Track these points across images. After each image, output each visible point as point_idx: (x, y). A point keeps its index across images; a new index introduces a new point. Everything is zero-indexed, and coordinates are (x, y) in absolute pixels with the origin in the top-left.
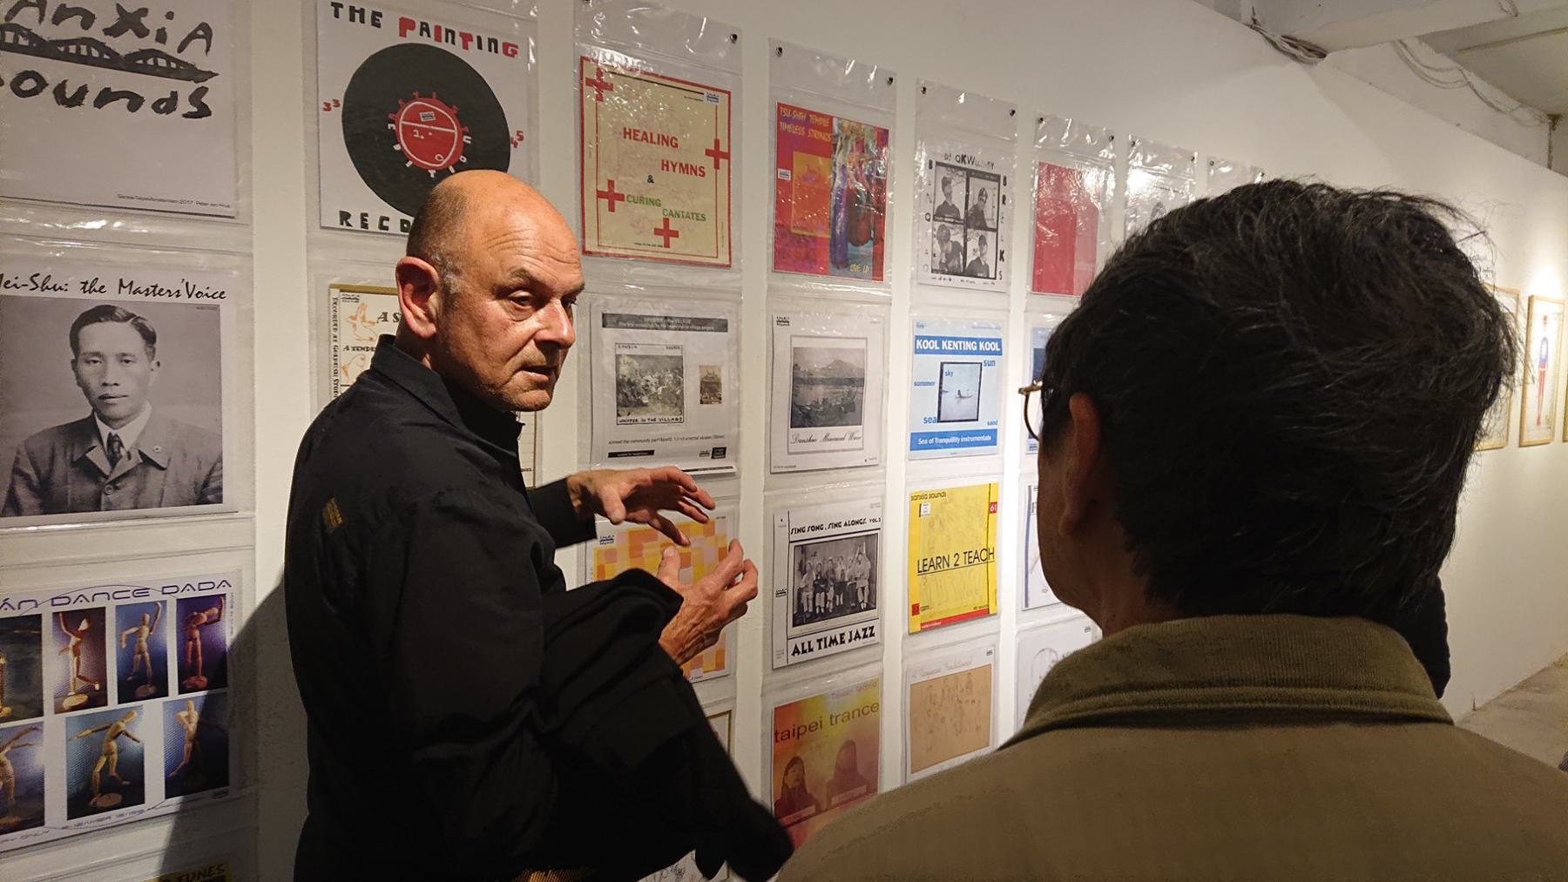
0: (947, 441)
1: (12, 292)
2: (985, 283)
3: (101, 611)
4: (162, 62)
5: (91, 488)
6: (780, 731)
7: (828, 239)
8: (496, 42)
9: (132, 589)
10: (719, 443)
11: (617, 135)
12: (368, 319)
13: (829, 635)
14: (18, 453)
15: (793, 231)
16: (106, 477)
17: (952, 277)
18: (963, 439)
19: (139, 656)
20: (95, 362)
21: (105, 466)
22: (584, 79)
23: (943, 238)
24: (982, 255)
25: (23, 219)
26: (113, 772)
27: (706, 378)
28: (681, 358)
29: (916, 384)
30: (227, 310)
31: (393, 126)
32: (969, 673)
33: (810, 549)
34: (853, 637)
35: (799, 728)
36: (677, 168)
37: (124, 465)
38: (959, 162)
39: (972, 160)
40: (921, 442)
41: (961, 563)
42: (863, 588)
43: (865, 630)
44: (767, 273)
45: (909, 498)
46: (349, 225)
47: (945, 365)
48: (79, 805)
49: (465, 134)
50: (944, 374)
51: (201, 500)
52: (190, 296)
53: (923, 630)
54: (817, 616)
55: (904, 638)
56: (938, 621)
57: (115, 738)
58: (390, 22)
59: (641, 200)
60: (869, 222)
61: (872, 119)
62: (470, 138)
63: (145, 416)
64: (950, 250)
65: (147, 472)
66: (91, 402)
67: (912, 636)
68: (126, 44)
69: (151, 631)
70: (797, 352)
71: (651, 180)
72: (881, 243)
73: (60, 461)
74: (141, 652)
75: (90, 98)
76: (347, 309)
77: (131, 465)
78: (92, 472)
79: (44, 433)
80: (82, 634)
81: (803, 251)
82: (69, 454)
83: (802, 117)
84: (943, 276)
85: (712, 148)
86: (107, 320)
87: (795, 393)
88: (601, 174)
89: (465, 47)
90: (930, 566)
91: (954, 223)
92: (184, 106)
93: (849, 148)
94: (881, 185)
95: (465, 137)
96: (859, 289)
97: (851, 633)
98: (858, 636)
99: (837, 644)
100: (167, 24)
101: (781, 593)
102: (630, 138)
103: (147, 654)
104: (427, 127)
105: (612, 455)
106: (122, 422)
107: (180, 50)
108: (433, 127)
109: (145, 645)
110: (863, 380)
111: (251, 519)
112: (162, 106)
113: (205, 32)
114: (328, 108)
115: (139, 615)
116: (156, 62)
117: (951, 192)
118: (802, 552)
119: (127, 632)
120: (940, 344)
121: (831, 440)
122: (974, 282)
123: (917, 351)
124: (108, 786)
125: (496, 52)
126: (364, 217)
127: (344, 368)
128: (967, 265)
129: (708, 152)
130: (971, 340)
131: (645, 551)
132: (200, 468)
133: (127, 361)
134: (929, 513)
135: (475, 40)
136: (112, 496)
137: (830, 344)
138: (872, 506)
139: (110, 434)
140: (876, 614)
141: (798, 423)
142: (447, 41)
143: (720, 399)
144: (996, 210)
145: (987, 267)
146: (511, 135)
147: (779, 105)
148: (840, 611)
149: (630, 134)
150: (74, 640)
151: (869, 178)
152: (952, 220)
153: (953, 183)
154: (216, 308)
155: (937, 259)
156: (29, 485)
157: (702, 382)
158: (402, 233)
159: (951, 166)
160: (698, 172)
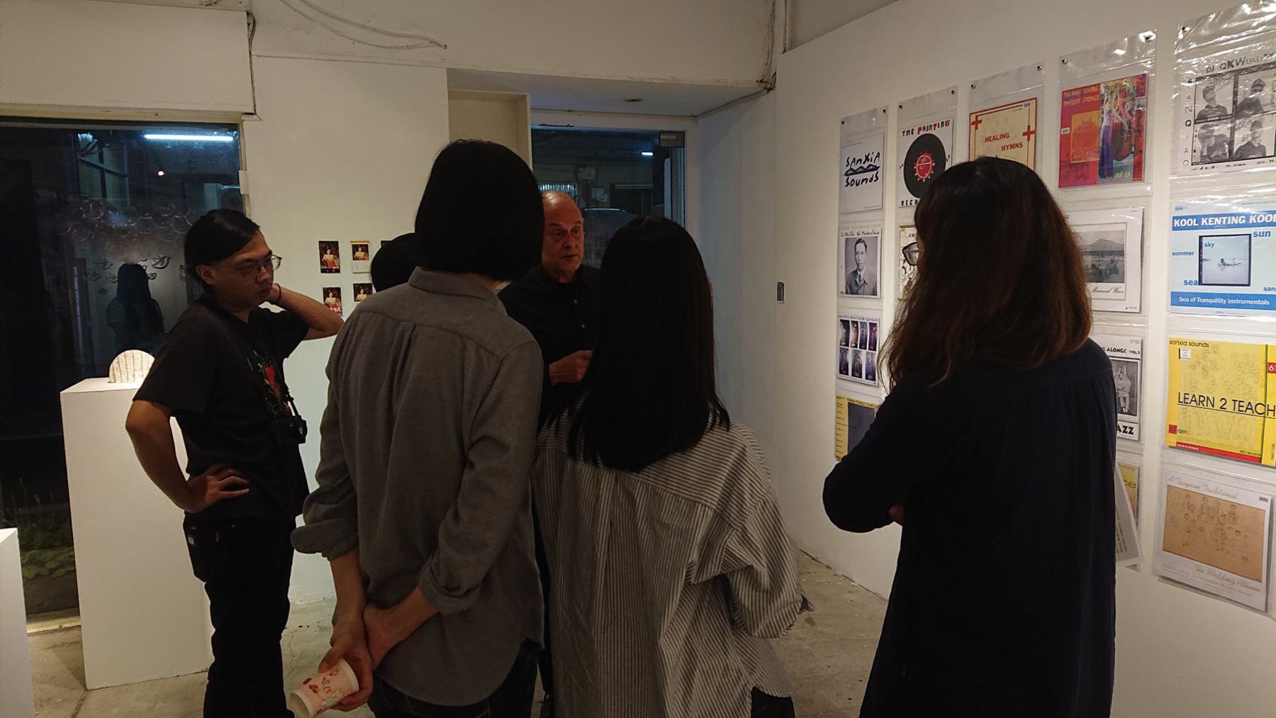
0: (1211, 301)
1: (850, 237)
7: (1096, 161)
15: (1072, 162)
18: (1230, 302)
21: (858, 282)
29: (1174, 254)
32: (1233, 505)
38: (1225, 68)
40: (1182, 300)
41: (1229, 406)
42: (1125, 398)
43: (1126, 427)
50: (1204, 246)
51: (874, 295)
56: (1197, 446)
58: (916, 131)
60: (1131, 141)
64: (1213, 143)
67: (1171, 449)
68: (865, 166)
76: (903, 233)
81: (1079, 173)
84: (1206, 166)
91: (1219, 120)
92: (875, 178)
94: (1140, 115)
110: (1123, 251)
115: (863, 324)
120: (1199, 221)
121: (1099, 291)
122: (1244, 165)
123: (1175, 229)
124: (857, 372)
129: (1024, 134)
136: (859, 291)
138: (1132, 341)
145: (1262, 149)
147: (1063, 92)
151: (1130, 112)
152: (1217, 118)
154: (877, 237)
155: (1198, 154)
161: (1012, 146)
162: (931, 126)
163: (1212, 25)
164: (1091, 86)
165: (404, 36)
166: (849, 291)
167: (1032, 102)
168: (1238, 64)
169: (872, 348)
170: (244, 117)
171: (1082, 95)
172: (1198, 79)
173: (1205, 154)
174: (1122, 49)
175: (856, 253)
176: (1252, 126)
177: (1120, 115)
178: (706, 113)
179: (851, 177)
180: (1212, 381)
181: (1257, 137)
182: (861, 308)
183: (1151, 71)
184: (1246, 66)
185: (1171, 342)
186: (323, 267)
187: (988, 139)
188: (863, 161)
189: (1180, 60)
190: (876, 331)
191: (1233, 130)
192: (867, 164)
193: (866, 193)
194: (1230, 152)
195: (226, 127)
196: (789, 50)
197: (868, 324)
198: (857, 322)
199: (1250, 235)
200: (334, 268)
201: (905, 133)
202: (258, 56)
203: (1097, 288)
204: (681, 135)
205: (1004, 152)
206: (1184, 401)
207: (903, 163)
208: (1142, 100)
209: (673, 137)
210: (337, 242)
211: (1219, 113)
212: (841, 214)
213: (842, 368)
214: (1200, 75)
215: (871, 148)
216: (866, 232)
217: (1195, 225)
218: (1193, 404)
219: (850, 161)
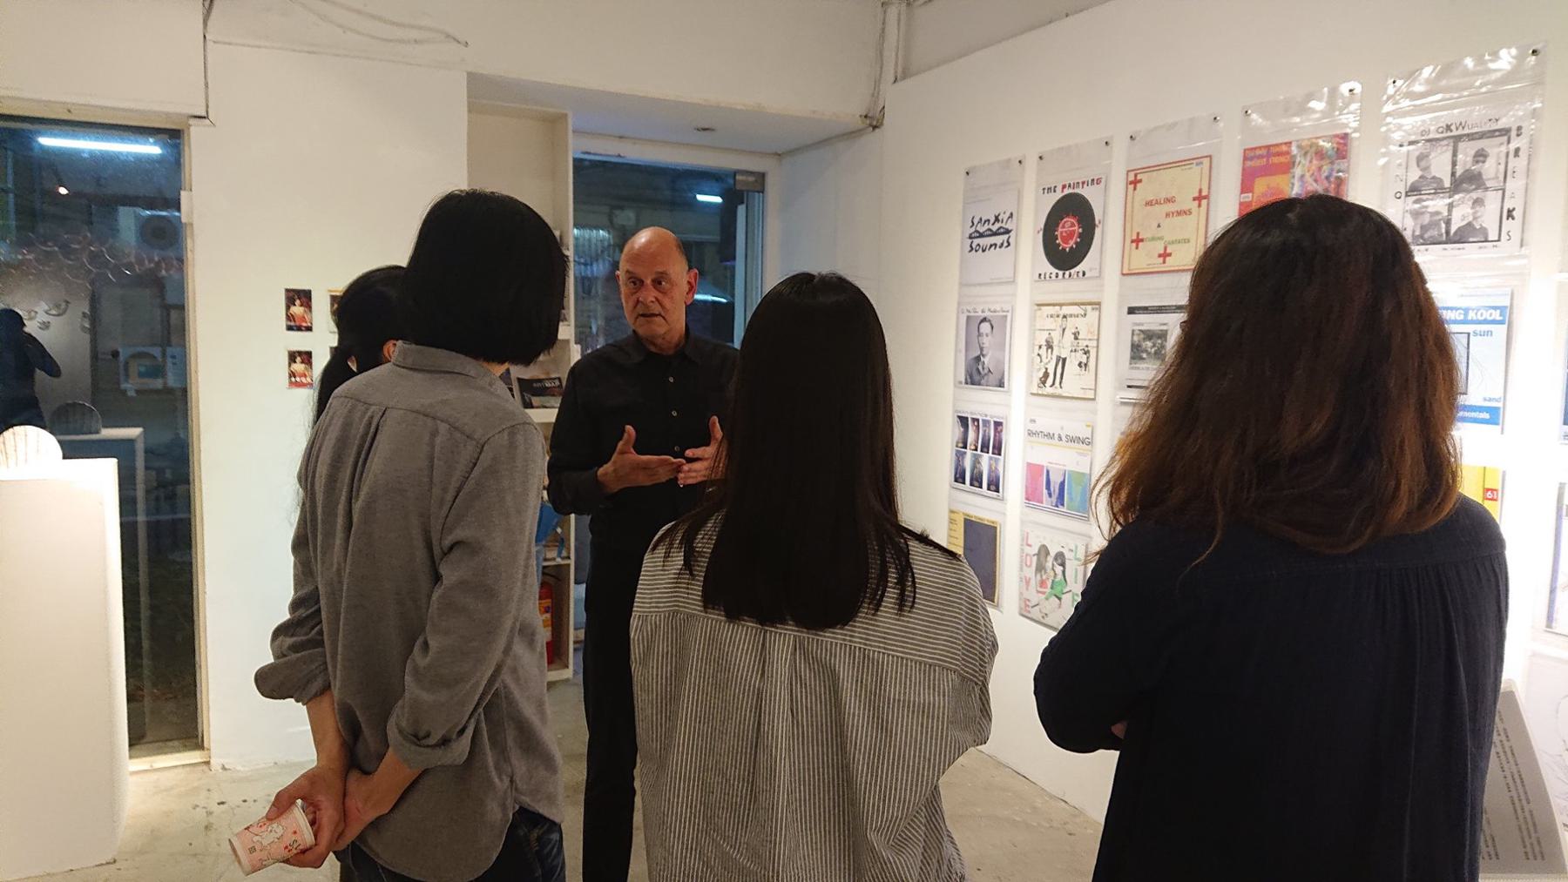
2: (1480, 248)
4: (1002, 230)
24: (1475, 218)
30: (1009, 315)
38: (1442, 132)
39: (1461, 125)
51: (1000, 386)
58: (1059, 189)
59: (1153, 239)
63: (989, 354)
68: (994, 228)
71: (1159, 226)
76: (1039, 313)
83: (1264, 152)
92: (1006, 244)
93: (1309, 158)
105: (1129, 387)
115: (986, 423)
122: (1463, 249)
128: (1452, 232)
129: (1194, 199)
130: (1457, 309)
136: (983, 381)
144: (1502, 167)
145: (1484, 231)
151: (1327, 178)
152: (1433, 191)
154: (1006, 316)
162: (1078, 183)
163: (1428, 81)
164: (1281, 144)
165: (412, 27)
166: (969, 380)
167: (1206, 160)
168: (1457, 129)
169: (996, 452)
170: (192, 121)
171: (1269, 155)
172: (1411, 143)
173: (1417, 233)
174: (1320, 100)
175: (980, 335)
176: (1474, 203)
177: (1316, 181)
178: (792, 152)
179: (976, 241)
181: (1479, 217)
182: (982, 402)
183: (1355, 130)
184: (1466, 131)
186: (289, 323)
187: (1149, 203)
188: (992, 221)
189: (1389, 119)
190: (1001, 431)
191: (1451, 206)
192: (997, 225)
193: (994, 262)
194: (1448, 232)
195: (166, 134)
196: (901, 80)
197: (992, 423)
198: (978, 420)
199: (1469, 334)
200: (304, 324)
201: (1046, 191)
202: (214, 42)
204: (762, 177)
205: (1168, 219)
207: (1042, 226)
208: (1342, 164)
209: (751, 179)
210: (310, 292)
211: (1435, 185)
212: (962, 285)
213: (958, 476)
214: (1413, 138)
215: (1002, 206)
216: (992, 310)
219: (976, 221)
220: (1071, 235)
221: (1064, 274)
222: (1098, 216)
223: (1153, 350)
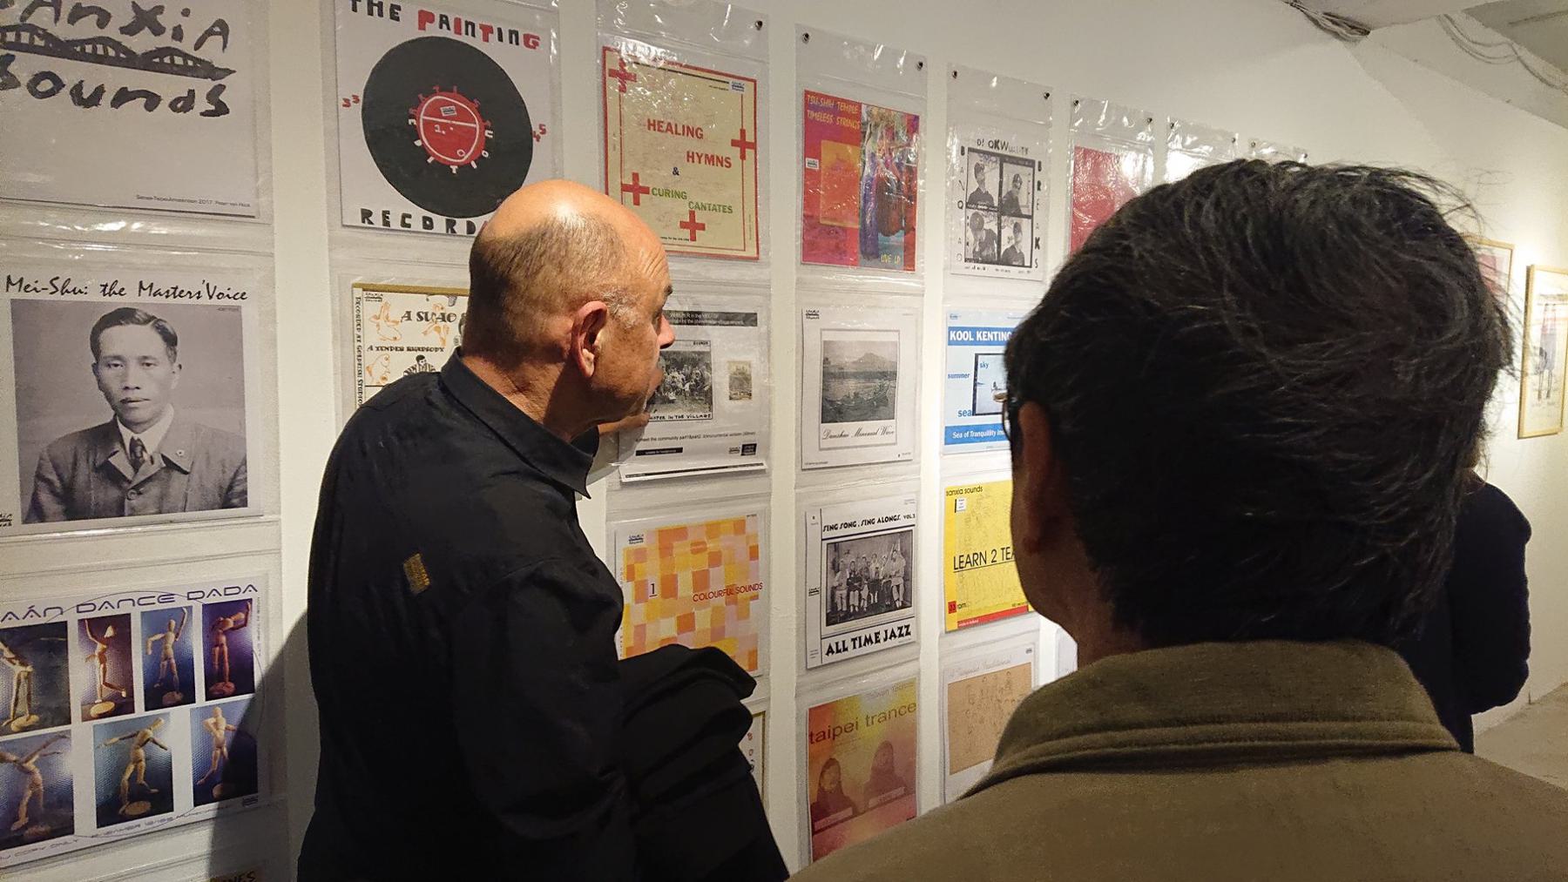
0: (982, 434)
1: (32, 296)
2: (1020, 272)
3: (128, 615)
4: (179, 60)
5: (114, 493)
6: (815, 732)
8: (516, 33)
9: (157, 595)
10: (748, 440)
11: (642, 127)
12: (391, 318)
13: (863, 634)
14: (41, 459)
16: (130, 482)
17: (986, 265)
19: (166, 663)
20: (116, 365)
21: (127, 471)
22: (607, 71)
23: (976, 226)
24: (1017, 243)
25: (46, 223)
26: (141, 780)
27: (735, 374)
28: (709, 353)
30: (249, 310)
31: (414, 121)
32: (1008, 672)
33: (844, 547)
34: (889, 636)
35: (834, 730)
36: (703, 159)
37: (148, 470)
39: (1005, 146)
40: (956, 436)
41: (999, 559)
42: (898, 586)
43: (900, 628)
44: (796, 265)
45: (944, 494)
46: (371, 223)
47: (980, 357)
48: (109, 813)
49: (486, 128)
50: (979, 366)
51: (226, 504)
52: (211, 297)
53: (960, 629)
54: (851, 616)
55: (940, 637)
56: (975, 619)
57: (143, 745)
58: (409, 15)
59: (667, 193)
61: (903, 105)
62: (492, 132)
65: (170, 477)
66: (114, 408)
68: (142, 43)
69: (176, 637)
70: (827, 345)
71: (676, 172)
72: (911, 232)
73: (82, 466)
74: (167, 658)
75: (108, 97)
76: (370, 308)
77: (153, 469)
78: (112, 475)
79: (65, 438)
80: (107, 642)
81: (833, 242)
82: (91, 459)
83: (829, 104)
84: (977, 265)
85: (738, 137)
86: (128, 323)
87: (825, 389)
88: (627, 166)
89: (486, 39)
90: (967, 563)
91: (988, 210)
92: (202, 104)
93: (879, 135)
94: (912, 173)
95: (487, 132)
96: (892, 280)
97: (886, 632)
98: (893, 635)
99: (872, 643)
100: (183, 21)
101: (813, 592)
102: (655, 130)
103: (173, 661)
104: (449, 122)
106: (146, 425)
107: (197, 48)
108: (454, 122)
109: (171, 652)
111: (277, 522)
112: (179, 105)
113: (221, 29)
114: (347, 104)
115: (164, 621)
116: (172, 60)
117: (984, 179)
118: (835, 550)
119: (153, 639)
120: (974, 336)
123: (950, 343)
124: (137, 794)
125: (517, 44)
126: (385, 214)
127: (368, 367)
129: (734, 143)
131: (675, 551)
132: (224, 472)
133: (148, 365)
134: (965, 508)
135: (496, 31)
136: (135, 501)
137: (861, 337)
139: (132, 439)
140: (911, 613)
141: (829, 419)
142: (467, 34)
143: (750, 395)
146: (533, 130)
148: (874, 609)
149: (654, 125)
150: (100, 647)
151: (899, 165)
152: (986, 208)
153: (986, 169)
154: (237, 309)
155: (971, 248)
156: (53, 492)
157: (731, 378)
158: (403, 229)
159: (984, 153)
160: (724, 163)
161: (710, 159)
180: (984, 532)
184: (1007, 153)
185: (948, 494)
187: (654, 125)
198: (122, 622)
203: (860, 430)
206: (959, 568)
211: (987, 202)
217: (972, 339)
218: (969, 565)
220: (465, 138)
221: (450, 225)
222: (537, 115)
223: (687, 385)
